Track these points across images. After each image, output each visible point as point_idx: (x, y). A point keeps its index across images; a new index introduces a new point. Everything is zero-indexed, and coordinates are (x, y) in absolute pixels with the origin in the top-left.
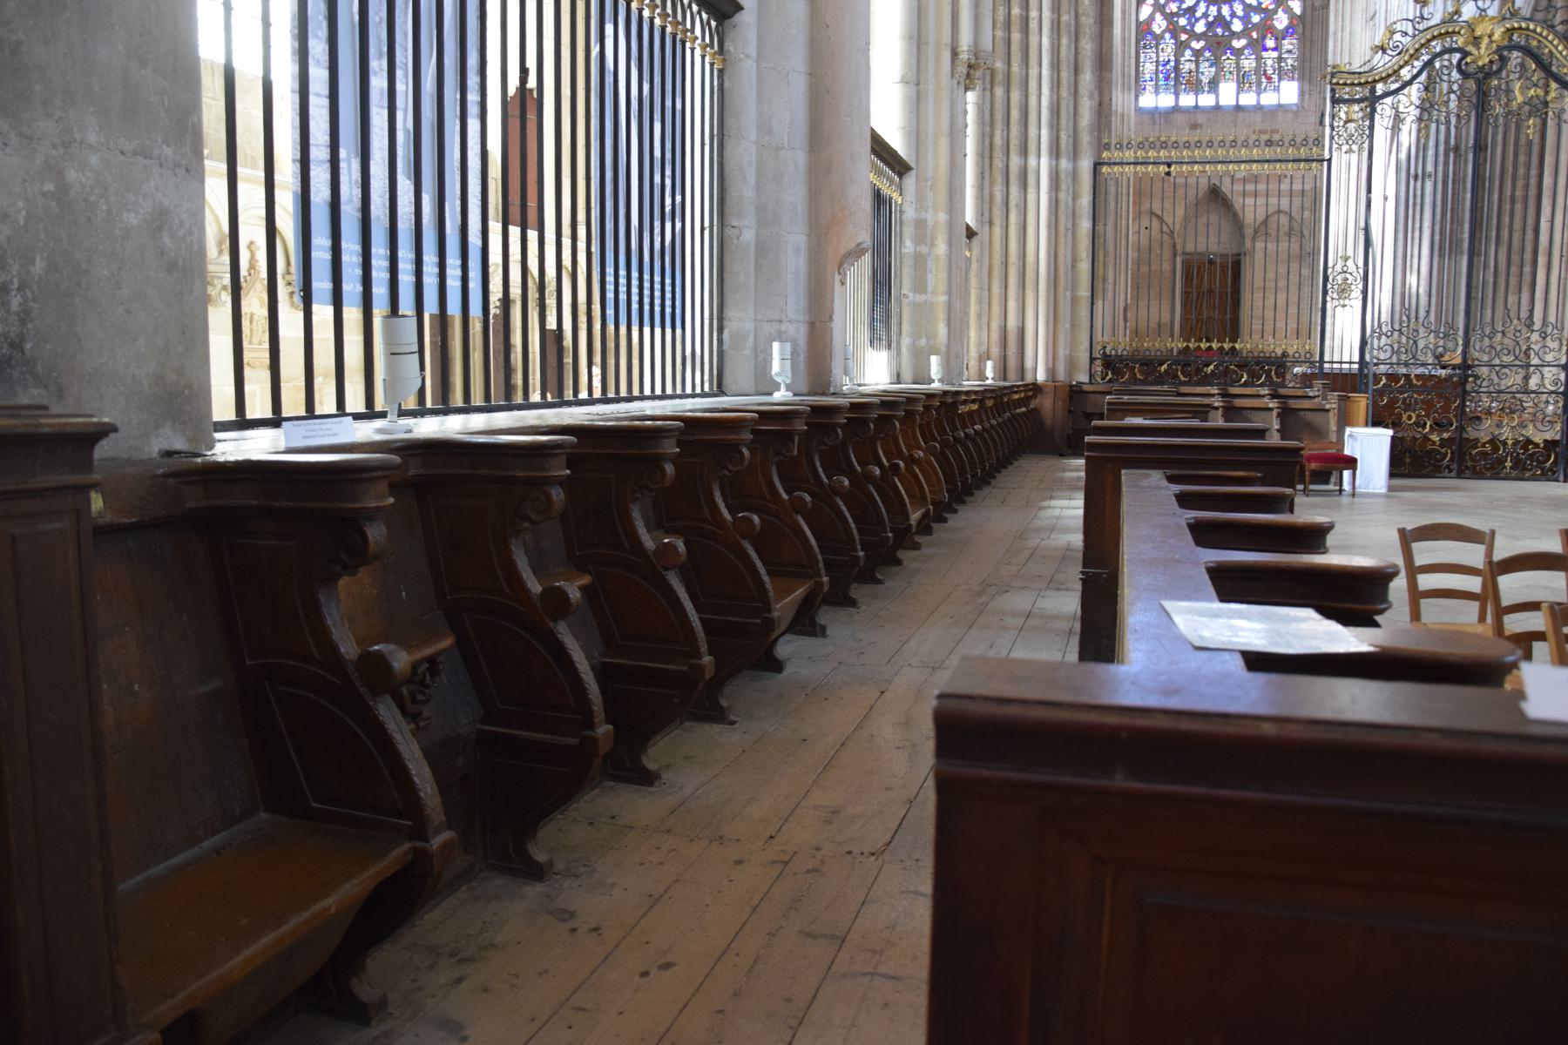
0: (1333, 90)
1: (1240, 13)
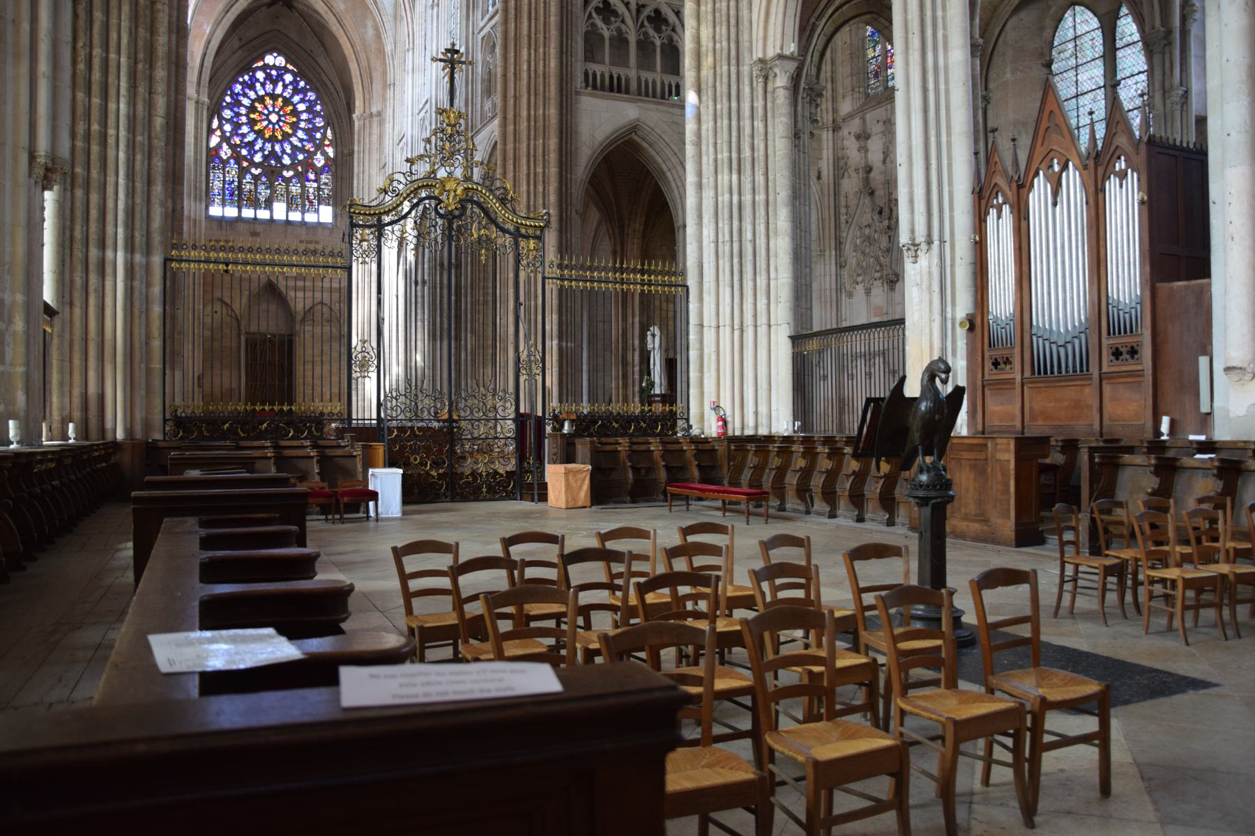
1: (288, 151)
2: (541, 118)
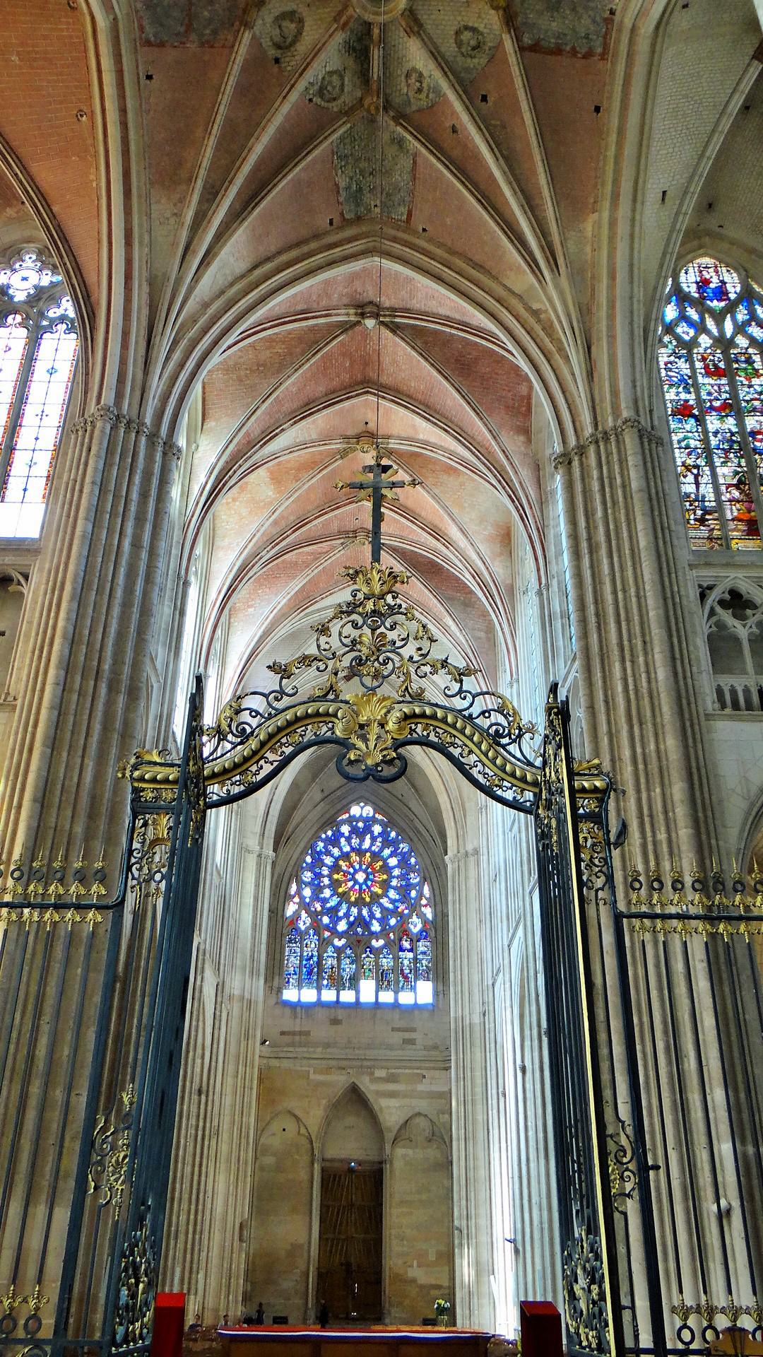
1: (378, 915)
2: (654, 755)
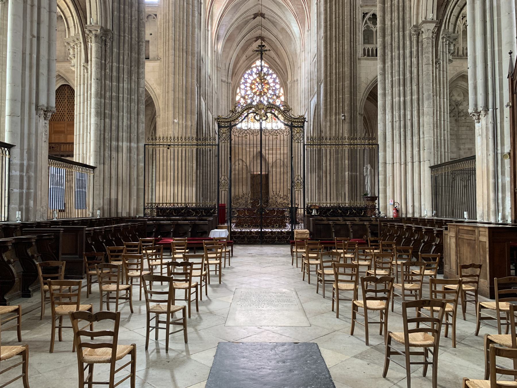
0: (218, 124)
2: (341, 72)
